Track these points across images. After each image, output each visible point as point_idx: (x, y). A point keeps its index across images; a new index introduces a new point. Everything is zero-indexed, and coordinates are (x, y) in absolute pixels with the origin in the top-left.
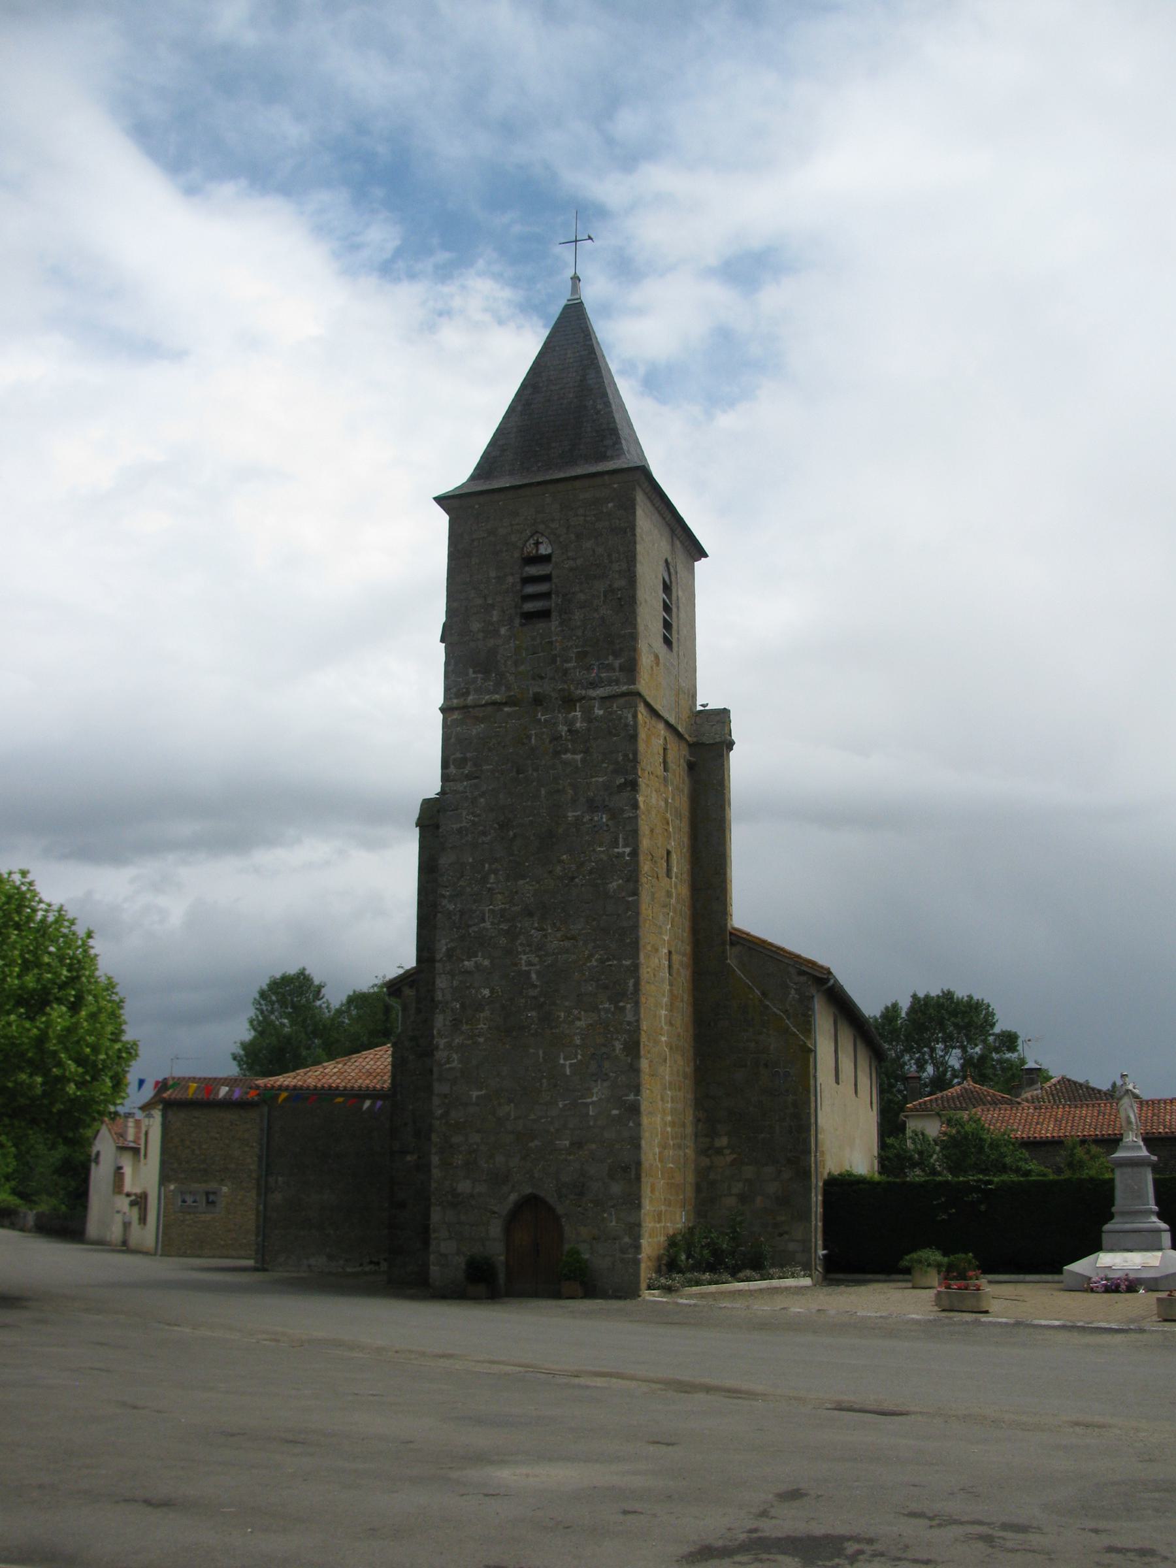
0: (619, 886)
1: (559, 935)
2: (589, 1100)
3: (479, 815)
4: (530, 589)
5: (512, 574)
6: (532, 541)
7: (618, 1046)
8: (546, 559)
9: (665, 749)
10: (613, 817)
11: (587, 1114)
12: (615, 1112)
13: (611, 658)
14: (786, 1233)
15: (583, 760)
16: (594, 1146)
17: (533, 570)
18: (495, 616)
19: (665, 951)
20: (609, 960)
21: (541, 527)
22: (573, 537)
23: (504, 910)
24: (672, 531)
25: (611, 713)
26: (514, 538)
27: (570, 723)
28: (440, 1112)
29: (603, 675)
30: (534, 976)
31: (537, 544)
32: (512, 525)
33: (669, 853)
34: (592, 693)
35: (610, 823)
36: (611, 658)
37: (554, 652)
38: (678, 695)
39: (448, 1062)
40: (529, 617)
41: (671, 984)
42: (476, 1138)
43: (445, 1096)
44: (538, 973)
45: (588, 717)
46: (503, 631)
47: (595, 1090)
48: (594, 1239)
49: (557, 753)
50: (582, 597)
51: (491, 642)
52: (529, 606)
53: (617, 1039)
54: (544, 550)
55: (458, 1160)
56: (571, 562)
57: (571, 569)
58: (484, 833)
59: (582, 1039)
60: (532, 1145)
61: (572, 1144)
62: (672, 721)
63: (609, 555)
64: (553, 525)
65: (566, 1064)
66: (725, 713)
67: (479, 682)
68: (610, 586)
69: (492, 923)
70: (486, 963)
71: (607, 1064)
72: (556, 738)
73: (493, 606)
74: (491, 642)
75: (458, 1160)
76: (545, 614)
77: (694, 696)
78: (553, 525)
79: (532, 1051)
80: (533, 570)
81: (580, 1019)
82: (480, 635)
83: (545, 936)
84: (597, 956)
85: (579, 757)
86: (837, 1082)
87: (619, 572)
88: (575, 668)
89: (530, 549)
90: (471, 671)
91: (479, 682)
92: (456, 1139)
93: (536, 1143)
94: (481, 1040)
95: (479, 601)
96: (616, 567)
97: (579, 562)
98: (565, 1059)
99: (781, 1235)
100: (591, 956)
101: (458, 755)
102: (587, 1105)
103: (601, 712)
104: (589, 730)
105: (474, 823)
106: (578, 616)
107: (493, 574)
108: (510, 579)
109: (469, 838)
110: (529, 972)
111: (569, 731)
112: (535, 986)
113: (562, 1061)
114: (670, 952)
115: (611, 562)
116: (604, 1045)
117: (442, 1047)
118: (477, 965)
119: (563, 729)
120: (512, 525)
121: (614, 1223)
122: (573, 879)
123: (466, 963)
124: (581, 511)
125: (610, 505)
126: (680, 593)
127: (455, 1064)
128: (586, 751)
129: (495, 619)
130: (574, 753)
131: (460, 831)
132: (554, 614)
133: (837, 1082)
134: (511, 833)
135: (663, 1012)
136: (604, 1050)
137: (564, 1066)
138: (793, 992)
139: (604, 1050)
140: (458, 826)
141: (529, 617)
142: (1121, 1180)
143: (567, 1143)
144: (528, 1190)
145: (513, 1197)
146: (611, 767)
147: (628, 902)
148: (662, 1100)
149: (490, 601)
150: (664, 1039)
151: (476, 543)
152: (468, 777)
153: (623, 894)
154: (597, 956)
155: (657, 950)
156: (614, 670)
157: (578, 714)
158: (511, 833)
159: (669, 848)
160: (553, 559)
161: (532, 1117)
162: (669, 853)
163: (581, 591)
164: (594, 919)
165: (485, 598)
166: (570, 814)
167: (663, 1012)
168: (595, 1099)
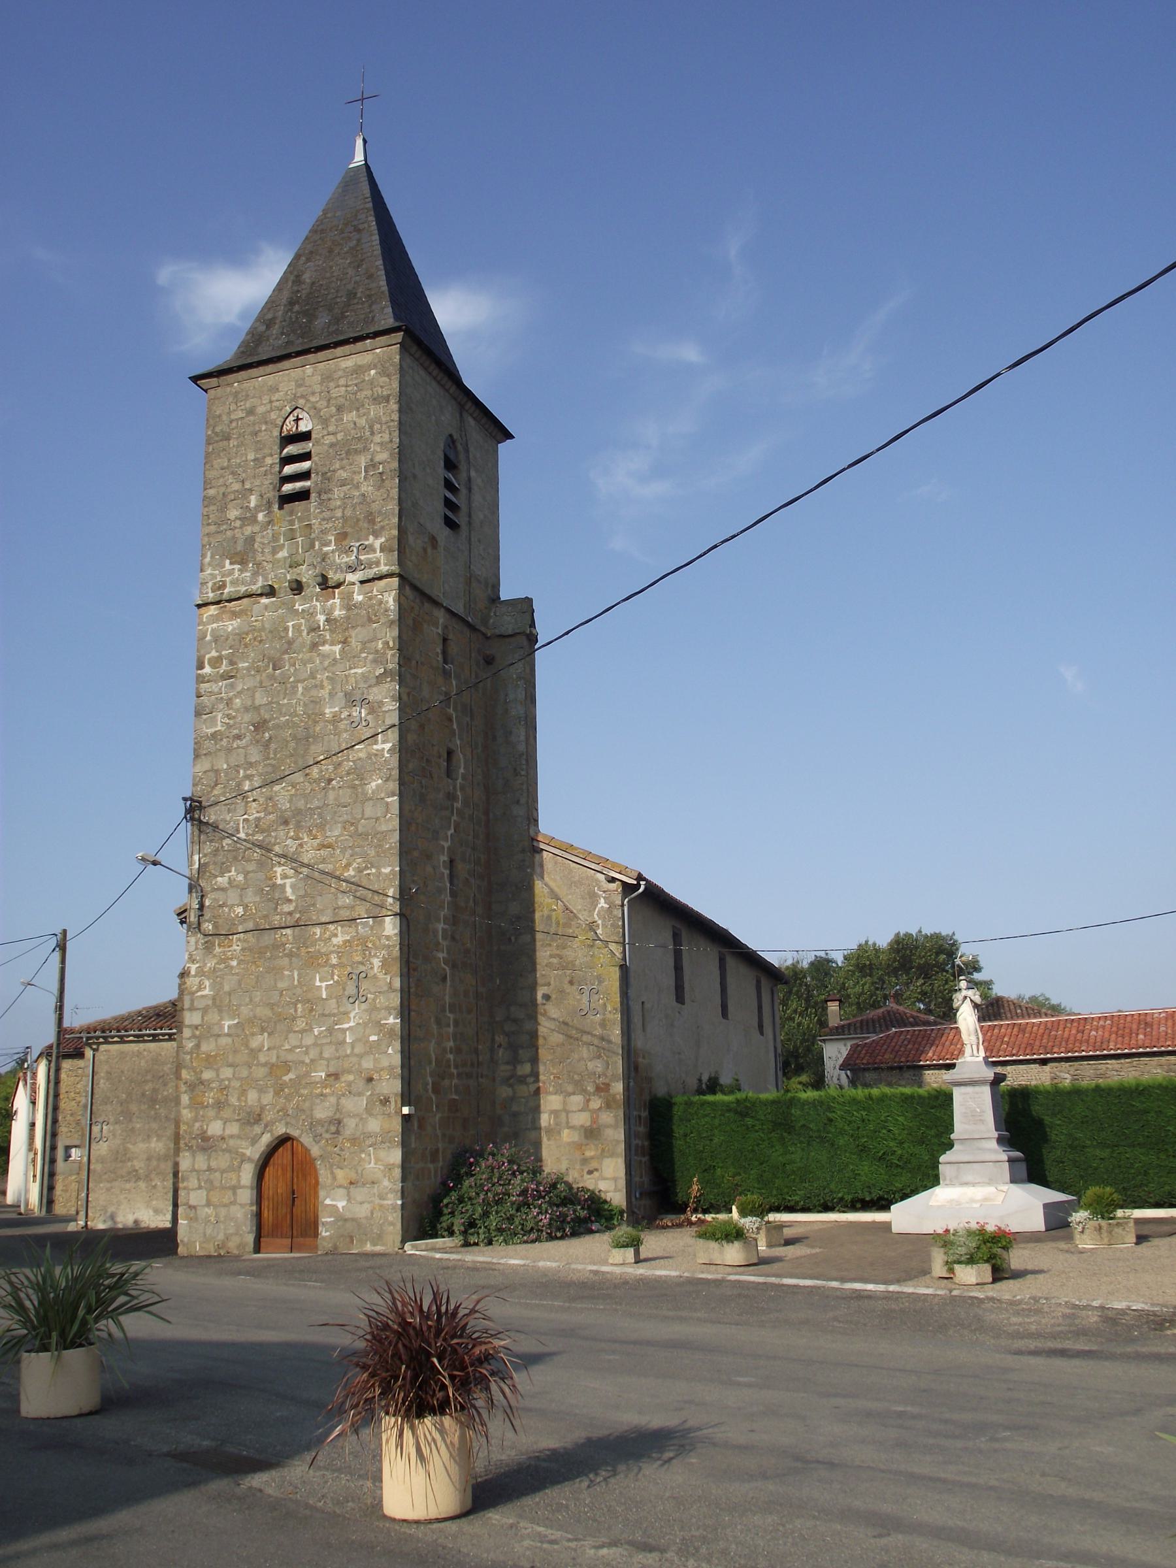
0: (377, 786)
1: (316, 842)
2: (346, 1026)
3: (234, 717)
4: (289, 469)
5: (272, 455)
6: (291, 418)
7: (376, 962)
8: (306, 436)
9: (445, 640)
10: (372, 711)
11: (344, 1041)
12: (374, 1038)
13: (371, 538)
14: (597, 1170)
15: (342, 651)
16: (351, 1077)
17: (291, 449)
18: (253, 501)
19: (444, 858)
20: (366, 868)
21: (301, 402)
22: (333, 409)
23: (258, 819)
24: (462, 407)
25: (370, 598)
26: (273, 416)
27: (328, 614)
28: (191, 1045)
29: (362, 557)
30: (289, 890)
31: (297, 420)
32: (271, 402)
33: (450, 753)
34: (351, 577)
35: (369, 718)
36: (371, 538)
37: (313, 536)
38: (468, 583)
39: (199, 989)
40: (286, 499)
41: (453, 894)
42: (227, 1072)
43: (196, 1027)
44: (293, 886)
45: (349, 606)
46: (260, 516)
47: (352, 1015)
48: (351, 1183)
49: (314, 646)
50: (343, 474)
51: (248, 530)
52: (288, 488)
53: (375, 955)
54: (304, 427)
55: (210, 1098)
56: (331, 437)
57: (332, 445)
58: (239, 737)
59: (339, 958)
60: (286, 1078)
61: (328, 1076)
62: (459, 608)
63: (371, 427)
64: (313, 399)
65: (322, 985)
66: (528, 601)
67: (237, 573)
68: (372, 460)
69: (247, 834)
70: (241, 878)
71: (364, 985)
72: (314, 629)
73: (251, 490)
74: (248, 530)
75: (210, 1098)
76: (303, 495)
77: (496, 587)
78: (313, 399)
79: (286, 973)
80: (291, 449)
81: (336, 935)
82: (238, 524)
83: (301, 845)
84: (355, 865)
85: (337, 648)
86: (680, 998)
87: (381, 444)
88: (333, 551)
89: (290, 427)
90: (228, 562)
91: (237, 573)
92: (207, 1075)
93: (291, 1076)
94: (234, 963)
95: (236, 486)
96: (377, 439)
97: (340, 436)
98: (321, 981)
99: (590, 1172)
100: (348, 865)
101: (214, 654)
102: (344, 1031)
103: (360, 598)
104: (348, 618)
105: (229, 726)
106: (337, 493)
107: (251, 456)
108: (269, 461)
109: (224, 742)
110: (284, 886)
111: (327, 620)
112: (290, 901)
113: (318, 983)
114: (451, 861)
115: (372, 433)
116: (362, 963)
117: (193, 972)
118: (230, 881)
119: (321, 618)
120: (271, 402)
121: (372, 1165)
122: (330, 781)
123: (219, 879)
124: (342, 382)
125: (373, 372)
126: (473, 474)
127: (206, 992)
128: (345, 642)
129: (252, 505)
130: (332, 644)
131: (214, 736)
132: (313, 496)
133: (680, 998)
134: (267, 735)
135: (440, 926)
136: (362, 968)
137: (320, 987)
138: (602, 900)
139: (362, 968)
140: (213, 730)
141: (286, 499)
142: (959, 1096)
143: (323, 1075)
144: (281, 1130)
145: (266, 1139)
146: (371, 657)
147: (387, 803)
148: (438, 1022)
149: (247, 486)
150: (441, 955)
151: (234, 424)
152: (226, 676)
153: (383, 795)
154: (355, 865)
155: (429, 857)
156: (374, 551)
157: (337, 601)
158: (267, 735)
159: (451, 746)
160: (313, 436)
161: (287, 1047)
162: (450, 753)
163: (342, 468)
164: (352, 824)
165: (243, 482)
166: (327, 711)
167: (440, 926)
168: (352, 1024)
